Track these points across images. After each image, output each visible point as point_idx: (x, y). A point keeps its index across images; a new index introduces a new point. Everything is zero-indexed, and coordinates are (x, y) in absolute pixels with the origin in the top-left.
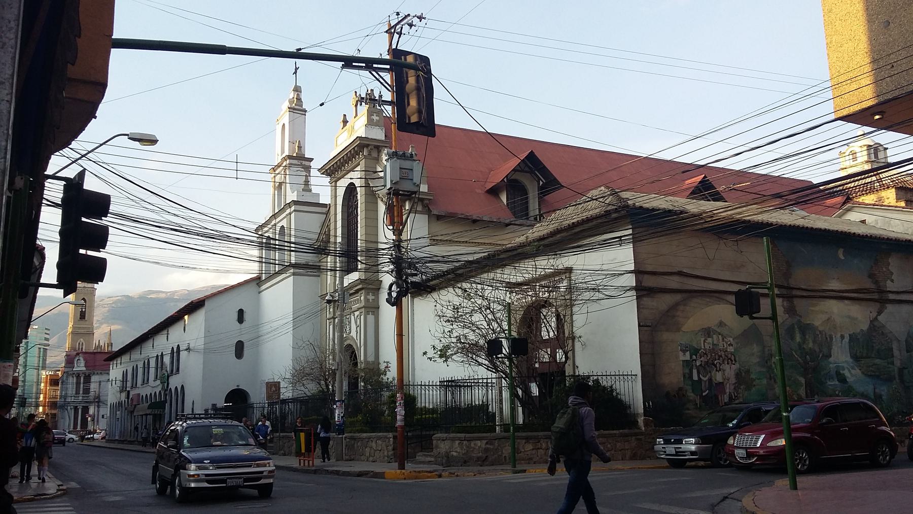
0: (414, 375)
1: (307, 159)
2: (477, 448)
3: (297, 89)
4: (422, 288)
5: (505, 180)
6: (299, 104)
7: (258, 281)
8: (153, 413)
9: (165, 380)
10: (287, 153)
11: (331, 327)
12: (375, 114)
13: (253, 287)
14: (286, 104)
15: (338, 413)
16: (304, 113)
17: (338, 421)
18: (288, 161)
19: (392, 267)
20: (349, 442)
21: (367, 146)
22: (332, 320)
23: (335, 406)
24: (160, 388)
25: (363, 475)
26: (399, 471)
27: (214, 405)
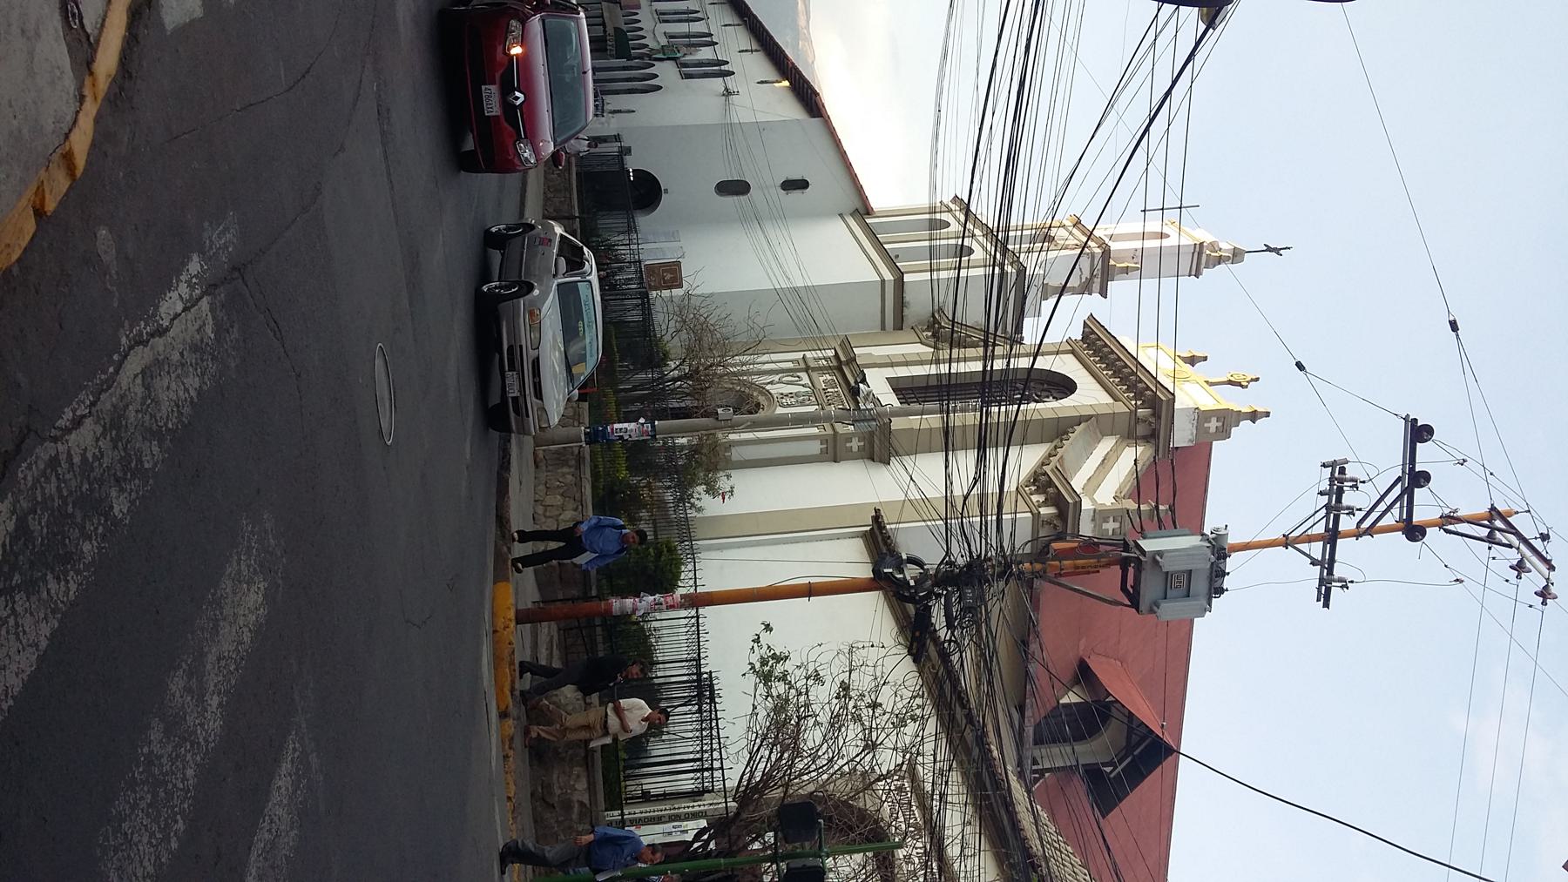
0: (710, 548)
1: (1105, 287)
2: (572, 783)
3: (1237, 255)
4: (917, 634)
5: (1110, 699)
6: (1210, 263)
7: (863, 210)
8: (608, 38)
9: (669, 54)
10: (1114, 246)
11: (790, 365)
12: (1220, 424)
13: (853, 203)
14: (1206, 237)
15: (630, 429)
16: (1193, 273)
17: (612, 429)
18: (1098, 251)
19: (961, 562)
20: (572, 453)
21: (1156, 414)
22: (804, 366)
23: (642, 420)
24: (653, 44)
25: (501, 527)
26: (512, 614)
27: (628, 151)
